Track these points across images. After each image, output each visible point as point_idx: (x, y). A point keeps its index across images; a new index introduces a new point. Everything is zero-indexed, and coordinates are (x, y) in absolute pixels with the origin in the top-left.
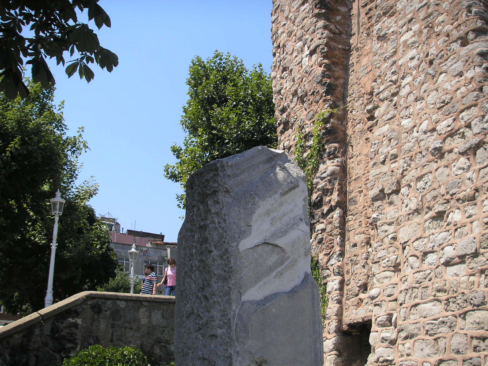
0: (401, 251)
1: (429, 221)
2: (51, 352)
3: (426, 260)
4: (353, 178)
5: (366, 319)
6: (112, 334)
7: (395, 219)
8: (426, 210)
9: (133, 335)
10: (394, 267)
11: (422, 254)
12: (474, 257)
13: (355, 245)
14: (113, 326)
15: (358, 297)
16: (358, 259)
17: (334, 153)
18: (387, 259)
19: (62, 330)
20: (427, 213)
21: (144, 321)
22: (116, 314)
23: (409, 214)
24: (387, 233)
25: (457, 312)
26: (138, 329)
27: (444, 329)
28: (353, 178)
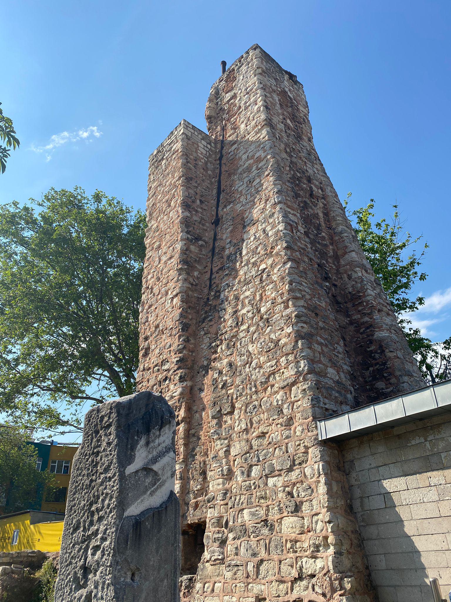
5: (202, 520)
12: (288, 472)
23: (240, 433)
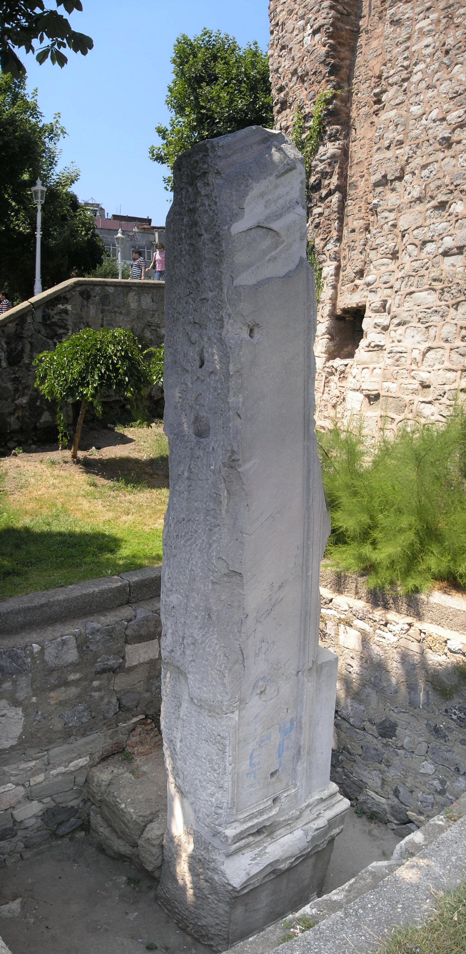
0: (400, 238)
1: (431, 210)
2: (44, 338)
3: (425, 249)
4: (355, 162)
5: (360, 304)
6: (103, 319)
7: (397, 206)
8: (429, 199)
9: (123, 319)
10: (392, 254)
11: (421, 242)
13: (353, 231)
14: (102, 312)
15: (353, 284)
16: (356, 245)
17: (335, 136)
18: (385, 246)
19: (53, 317)
20: (429, 202)
21: (133, 305)
22: (105, 299)
23: (411, 202)
24: (387, 220)
25: (450, 302)
26: (128, 314)
27: (436, 318)
28: (355, 162)
